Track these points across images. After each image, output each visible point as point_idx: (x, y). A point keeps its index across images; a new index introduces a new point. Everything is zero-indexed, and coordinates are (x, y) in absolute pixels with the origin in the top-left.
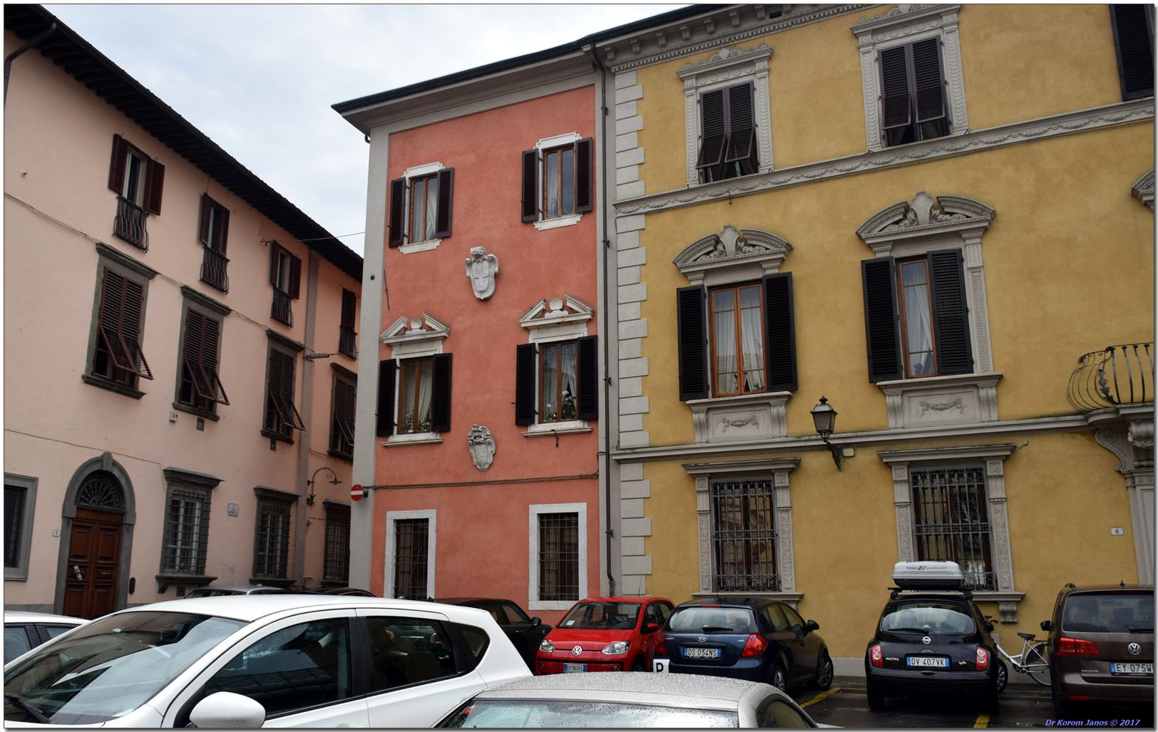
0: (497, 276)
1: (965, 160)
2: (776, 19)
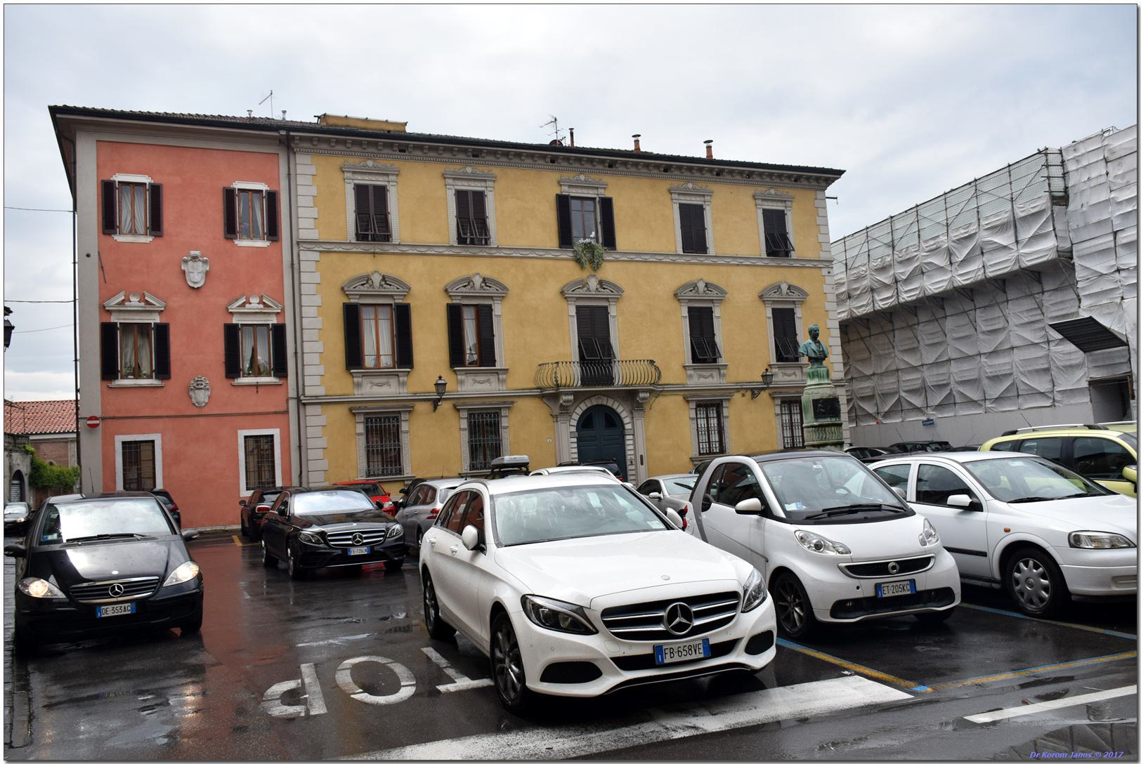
0: (207, 273)
1: (495, 260)
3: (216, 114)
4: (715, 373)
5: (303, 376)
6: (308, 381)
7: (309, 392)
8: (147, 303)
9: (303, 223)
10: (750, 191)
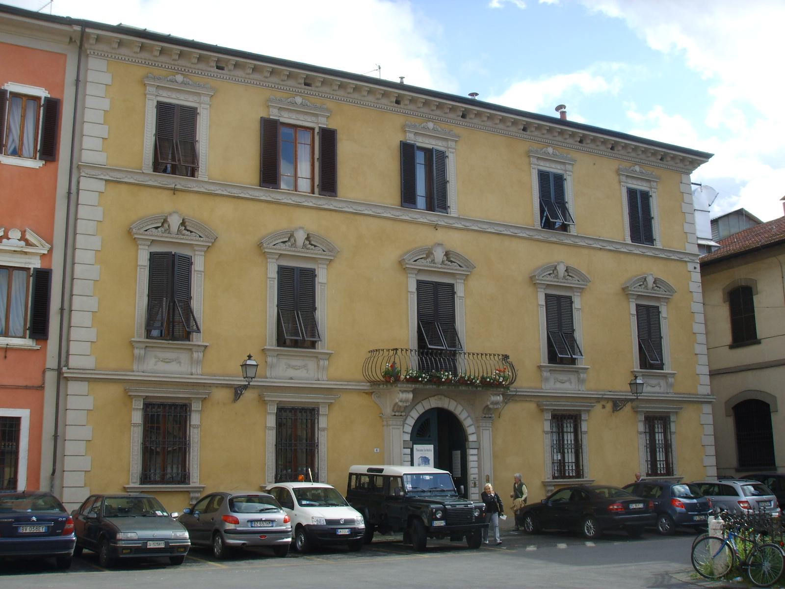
1: (322, 213)
3: (215, 44)
4: (573, 377)
5: (68, 341)
6: (74, 348)
7: (74, 362)
8: (28, 243)
9: (87, 143)
10: (614, 165)
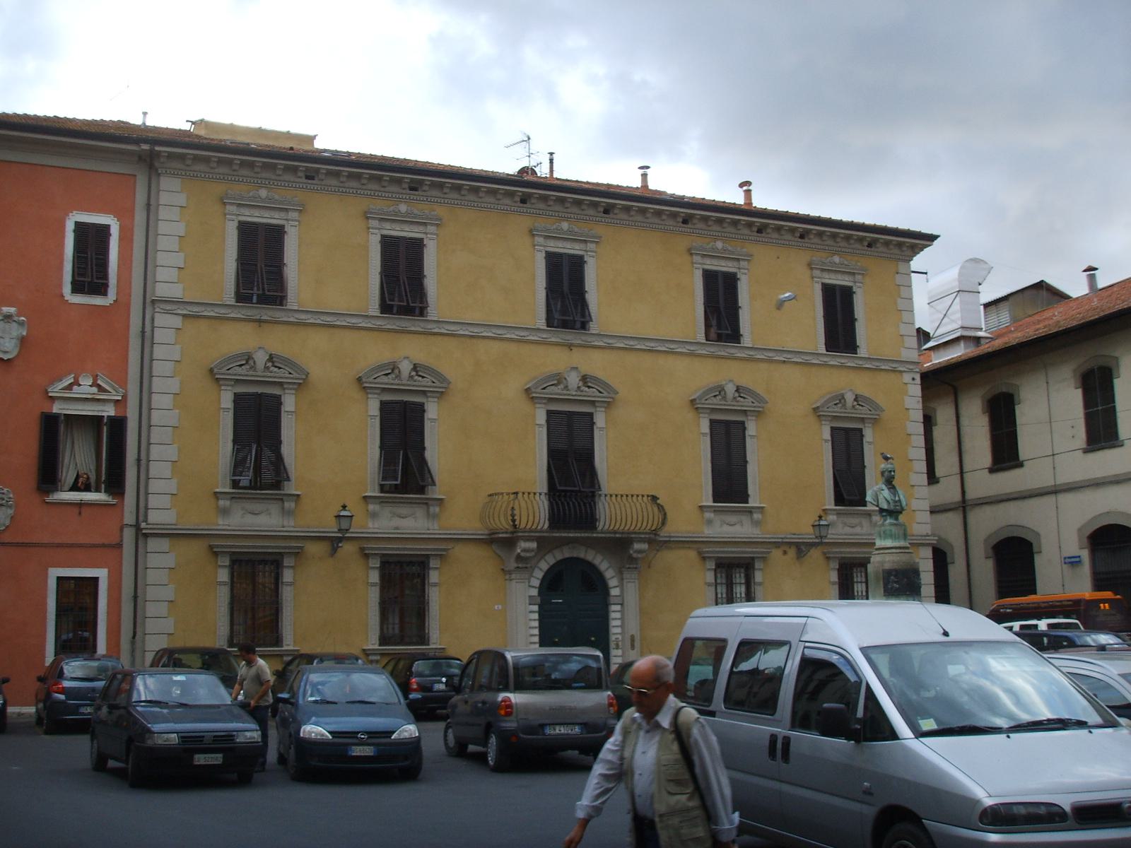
0: (23, 341)
1: (432, 338)
2: (310, 181)
5: (147, 494)
6: (153, 501)
7: (154, 517)
9: (162, 274)
10: (805, 256)
